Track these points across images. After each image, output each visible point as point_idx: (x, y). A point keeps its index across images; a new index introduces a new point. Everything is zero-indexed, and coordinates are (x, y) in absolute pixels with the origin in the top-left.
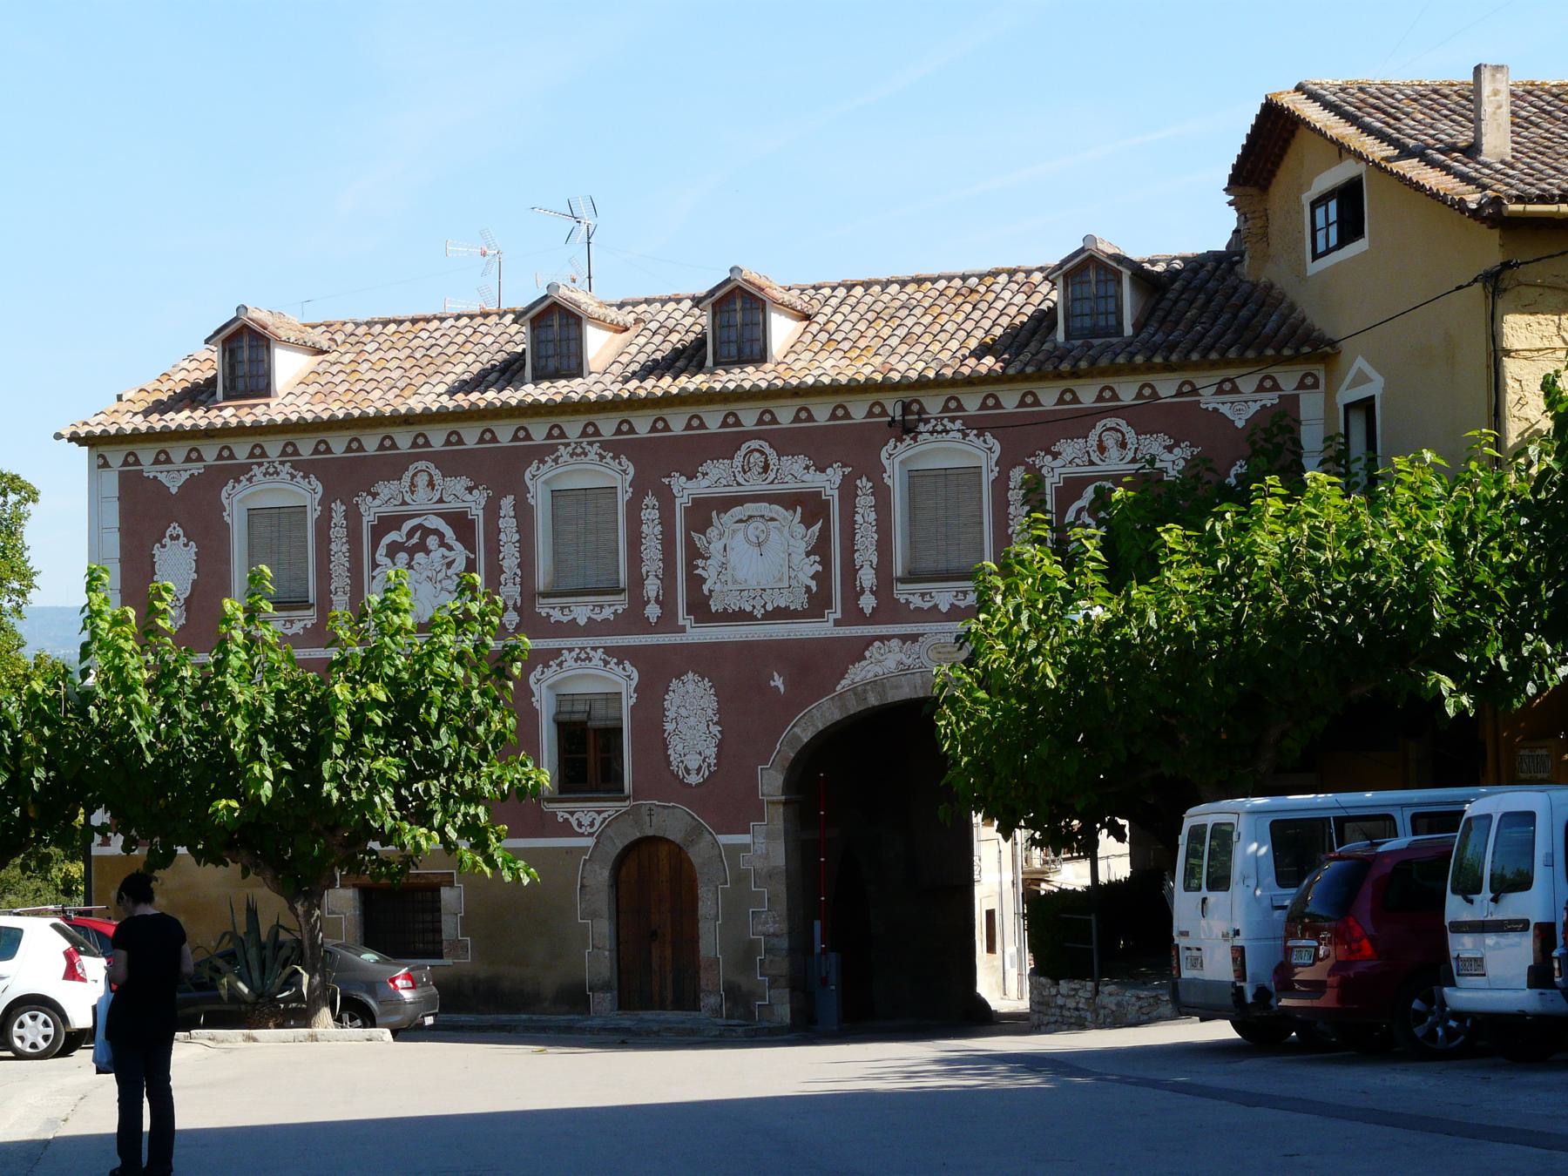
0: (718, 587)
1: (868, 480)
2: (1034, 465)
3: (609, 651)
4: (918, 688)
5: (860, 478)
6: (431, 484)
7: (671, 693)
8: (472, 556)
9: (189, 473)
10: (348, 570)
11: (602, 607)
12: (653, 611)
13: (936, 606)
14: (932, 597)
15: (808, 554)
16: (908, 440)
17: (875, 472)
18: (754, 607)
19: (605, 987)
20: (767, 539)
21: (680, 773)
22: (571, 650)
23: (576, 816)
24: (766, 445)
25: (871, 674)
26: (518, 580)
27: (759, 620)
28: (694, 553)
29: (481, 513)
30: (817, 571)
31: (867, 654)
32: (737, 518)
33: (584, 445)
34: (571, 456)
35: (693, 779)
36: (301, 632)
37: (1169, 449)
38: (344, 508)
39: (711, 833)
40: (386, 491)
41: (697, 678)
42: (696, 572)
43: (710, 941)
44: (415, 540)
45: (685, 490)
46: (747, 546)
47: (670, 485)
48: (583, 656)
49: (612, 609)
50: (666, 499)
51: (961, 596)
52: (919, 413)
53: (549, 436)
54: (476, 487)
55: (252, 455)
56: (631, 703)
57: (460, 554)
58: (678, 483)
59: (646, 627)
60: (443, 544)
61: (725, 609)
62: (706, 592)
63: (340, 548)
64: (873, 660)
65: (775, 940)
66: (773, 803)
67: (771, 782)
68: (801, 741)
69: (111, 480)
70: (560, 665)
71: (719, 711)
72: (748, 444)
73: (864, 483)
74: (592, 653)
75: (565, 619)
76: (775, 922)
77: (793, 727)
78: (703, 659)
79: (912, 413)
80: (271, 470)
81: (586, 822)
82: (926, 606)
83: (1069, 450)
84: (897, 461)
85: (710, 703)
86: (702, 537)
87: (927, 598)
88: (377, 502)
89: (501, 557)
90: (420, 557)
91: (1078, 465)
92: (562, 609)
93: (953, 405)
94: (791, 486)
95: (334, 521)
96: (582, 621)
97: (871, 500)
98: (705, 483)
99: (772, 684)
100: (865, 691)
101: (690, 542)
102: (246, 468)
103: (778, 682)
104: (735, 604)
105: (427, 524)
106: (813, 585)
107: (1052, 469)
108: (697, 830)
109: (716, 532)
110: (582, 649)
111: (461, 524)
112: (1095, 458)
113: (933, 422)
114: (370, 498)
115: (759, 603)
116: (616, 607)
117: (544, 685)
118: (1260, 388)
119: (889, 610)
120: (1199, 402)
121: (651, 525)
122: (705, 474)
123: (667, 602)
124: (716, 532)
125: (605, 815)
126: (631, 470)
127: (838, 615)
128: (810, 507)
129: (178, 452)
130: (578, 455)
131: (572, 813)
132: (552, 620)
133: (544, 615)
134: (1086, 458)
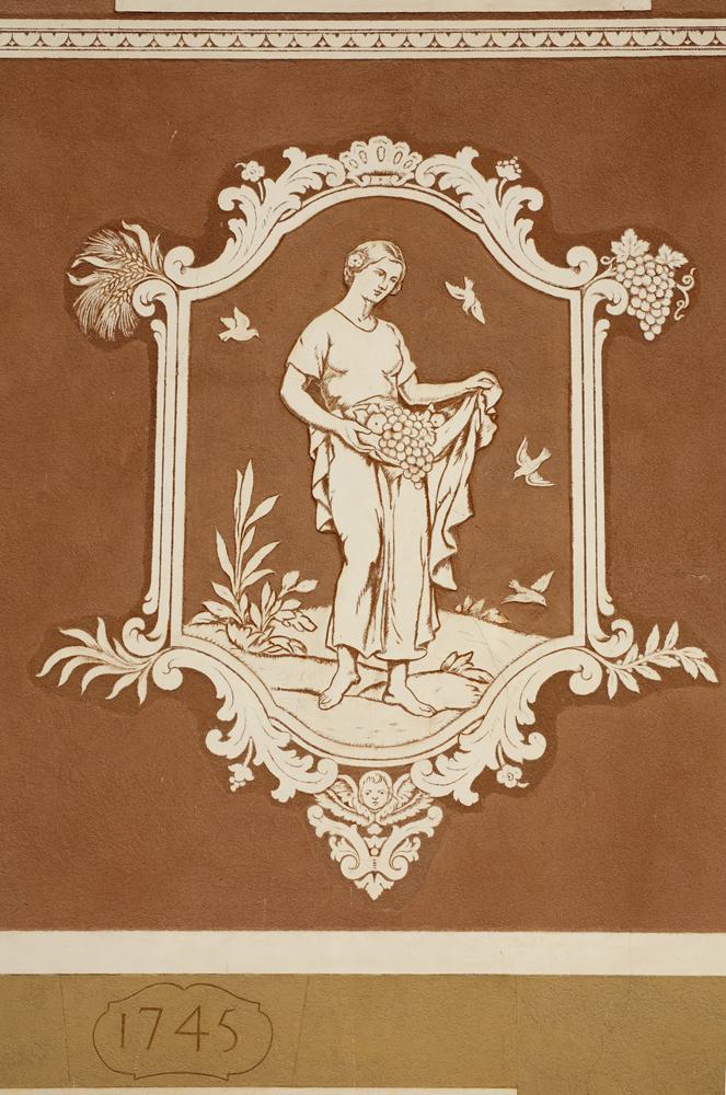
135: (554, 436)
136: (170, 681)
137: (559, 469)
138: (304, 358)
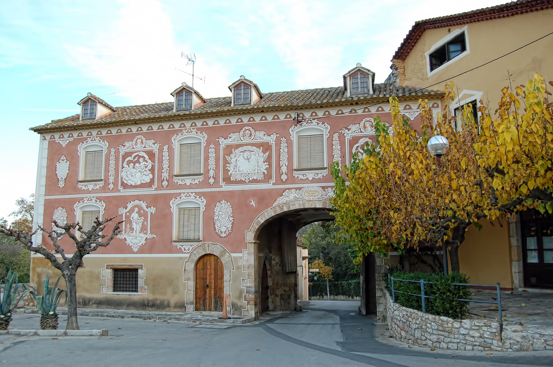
1: (285, 138)
2: (342, 133)
4: (301, 205)
5: (282, 138)
6: (142, 142)
7: (217, 207)
8: (154, 164)
9: (69, 141)
11: (195, 180)
12: (212, 181)
14: (306, 175)
15: (264, 162)
16: (299, 126)
17: (288, 136)
18: (245, 179)
19: (191, 303)
21: (219, 233)
22: (184, 193)
23: (183, 247)
24: (251, 128)
26: (168, 171)
27: (247, 183)
28: (226, 162)
31: (284, 194)
32: (240, 151)
33: (191, 129)
35: (223, 235)
39: (229, 253)
43: (228, 290)
44: (136, 160)
45: (223, 143)
47: (219, 141)
49: (198, 180)
50: (217, 145)
52: (302, 117)
53: (180, 127)
54: (156, 143)
55: (88, 135)
56: (203, 210)
57: (150, 164)
58: (221, 140)
59: (210, 186)
62: (230, 174)
63: (112, 162)
64: (286, 196)
65: (250, 289)
67: (250, 236)
68: (260, 222)
69: (46, 143)
73: (283, 139)
74: (191, 194)
75: (183, 184)
76: (250, 283)
77: (258, 218)
78: (228, 196)
79: (300, 117)
80: (93, 139)
81: (187, 249)
82: (304, 178)
83: (354, 128)
84: (295, 132)
85: (230, 210)
86: (229, 157)
87: (305, 176)
88: (125, 148)
89: (163, 164)
90: (137, 165)
91: (357, 133)
92: (182, 180)
93: (314, 114)
94: (259, 141)
95: (111, 154)
98: (230, 140)
99: (251, 204)
100: (283, 206)
101: (225, 159)
102: (86, 139)
103: (253, 203)
104: (239, 178)
106: (266, 172)
107: (348, 134)
108: (224, 252)
111: (151, 155)
112: (362, 130)
115: (247, 178)
116: (199, 180)
119: (291, 180)
125: (193, 246)
126: (206, 137)
127: (274, 182)
128: (266, 147)
129: (66, 135)
130: (189, 132)
131: (182, 246)
132: (178, 184)
135: (147, 221)
136: (124, 238)
137: (147, 223)
138: (132, 216)
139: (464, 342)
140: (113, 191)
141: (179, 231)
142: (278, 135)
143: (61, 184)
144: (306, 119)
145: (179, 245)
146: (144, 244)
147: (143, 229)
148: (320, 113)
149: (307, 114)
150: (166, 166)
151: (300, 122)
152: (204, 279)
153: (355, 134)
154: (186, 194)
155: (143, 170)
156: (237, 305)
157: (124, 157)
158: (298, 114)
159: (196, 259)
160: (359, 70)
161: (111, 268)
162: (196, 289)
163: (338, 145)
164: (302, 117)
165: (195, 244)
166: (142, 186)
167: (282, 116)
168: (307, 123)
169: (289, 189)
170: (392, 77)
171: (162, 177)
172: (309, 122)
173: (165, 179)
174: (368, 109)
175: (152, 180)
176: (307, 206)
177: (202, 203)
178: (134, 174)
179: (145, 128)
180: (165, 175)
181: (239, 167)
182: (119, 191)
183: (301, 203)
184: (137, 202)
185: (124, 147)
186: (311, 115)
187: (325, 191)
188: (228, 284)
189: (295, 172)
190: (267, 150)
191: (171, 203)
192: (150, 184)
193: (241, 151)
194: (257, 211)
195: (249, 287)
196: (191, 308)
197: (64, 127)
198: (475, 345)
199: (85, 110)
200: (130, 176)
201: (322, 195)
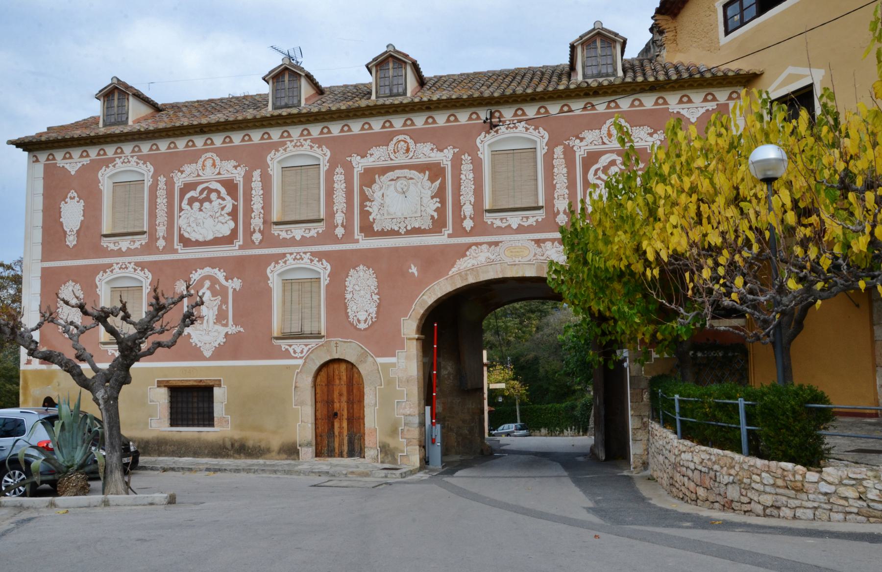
0: (378, 217)
1: (469, 155)
3: (313, 254)
5: (464, 154)
6: (214, 165)
10: (166, 213)
11: (310, 230)
12: (340, 231)
13: (509, 226)
15: (432, 198)
17: (473, 151)
18: (400, 228)
19: (308, 445)
20: (408, 190)
22: (291, 254)
23: (293, 347)
25: (470, 265)
26: (261, 215)
27: (401, 234)
28: (364, 198)
29: (241, 180)
30: (438, 207)
33: (302, 141)
34: (294, 147)
35: (362, 326)
36: (139, 247)
37: (651, 135)
38: (165, 179)
40: (189, 169)
41: (365, 268)
42: (366, 209)
43: (371, 419)
44: (204, 195)
45: (359, 164)
46: (396, 194)
48: (298, 257)
50: (349, 169)
51: (525, 220)
52: (499, 118)
53: (282, 136)
54: (239, 166)
55: (116, 153)
57: (229, 203)
59: (336, 240)
60: (219, 197)
61: (383, 229)
63: (162, 201)
65: (411, 418)
66: (410, 339)
67: (410, 328)
69: (39, 169)
70: (285, 262)
71: (378, 287)
72: (397, 137)
73: (466, 157)
74: (303, 256)
75: (288, 237)
76: (410, 408)
78: (369, 258)
79: (496, 118)
80: (126, 160)
81: (298, 350)
82: (504, 225)
83: (590, 136)
84: (486, 144)
85: (373, 282)
87: (504, 221)
88: (184, 175)
89: (252, 203)
90: (206, 204)
92: (287, 231)
93: (520, 112)
94: (422, 160)
95: (159, 186)
96: (298, 238)
97: (471, 167)
98: (372, 159)
99: (410, 271)
100: (466, 275)
101: (362, 193)
102: (112, 160)
103: (414, 270)
105: (211, 187)
106: (435, 215)
108: (364, 356)
109: (378, 186)
110: (298, 253)
112: (605, 140)
113: (508, 122)
114: (180, 173)
115: (402, 225)
117: (275, 274)
118: (705, 100)
119: (481, 228)
120: (668, 108)
121: (339, 183)
122: (371, 155)
123: (348, 226)
124: (378, 186)
126: (329, 154)
127: (450, 232)
128: (434, 171)
129: (76, 153)
130: (298, 146)
131: (290, 346)
132: (281, 237)
133: (276, 234)
134: (600, 141)
135: (227, 303)
137: (227, 307)
139: (828, 507)
140: (165, 250)
141: (283, 321)
142: (456, 150)
143: (71, 241)
144: (505, 122)
145: (284, 344)
146: (222, 344)
147: (221, 318)
148: (531, 111)
149: (508, 113)
150: (257, 204)
151: (496, 126)
152: (329, 402)
153: (592, 148)
154: (295, 254)
155: (218, 214)
156: (389, 446)
157: (183, 192)
158: (491, 112)
159: (315, 368)
160: (599, 34)
161: (165, 386)
162: (316, 419)
163: (564, 166)
164: (499, 118)
165: (313, 343)
166: (217, 241)
167: (463, 117)
168: (507, 129)
169: (477, 244)
170: (652, 47)
171: (252, 227)
172: (511, 126)
173: (257, 229)
174: (616, 103)
175: (234, 232)
176: (509, 274)
177: (324, 269)
178: (201, 221)
179: (218, 140)
180: (257, 222)
181: (388, 206)
182: (175, 251)
183: (499, 270)
184: (208, 271)
185: (182, 174)
186: (515, 115)
187: (539, 246)
188: (373, 411)
189: (488, 215)
190: (437, 175)
191: (268, 271)
192: (229, 239)
193: (391, 178)
194: (421, 284)
195: (409, 415)
196: (307, 453)
197: (72, 139)
198: (851, 513)
199: (107, 108)
200: (194, 225)
201: (535, 254)
